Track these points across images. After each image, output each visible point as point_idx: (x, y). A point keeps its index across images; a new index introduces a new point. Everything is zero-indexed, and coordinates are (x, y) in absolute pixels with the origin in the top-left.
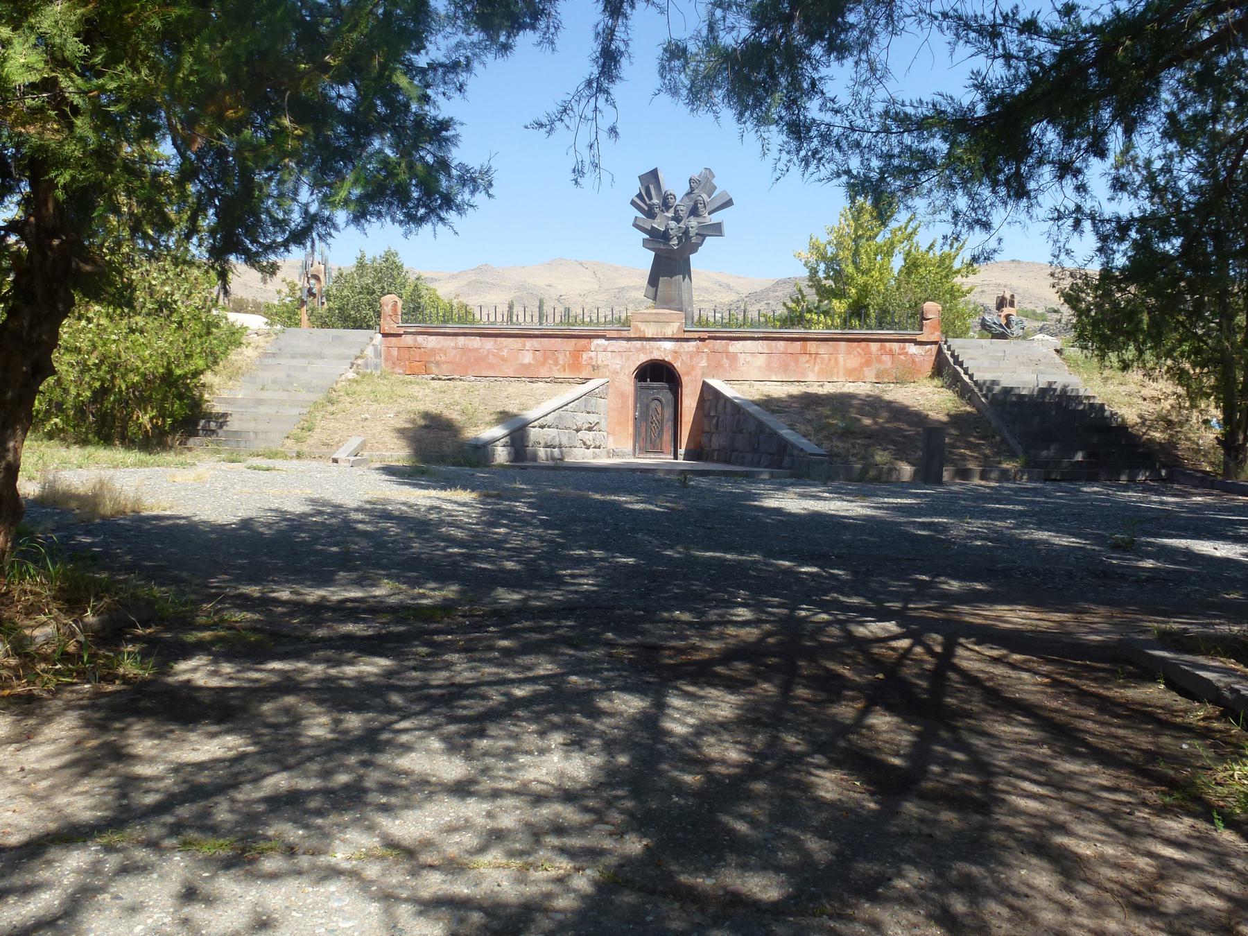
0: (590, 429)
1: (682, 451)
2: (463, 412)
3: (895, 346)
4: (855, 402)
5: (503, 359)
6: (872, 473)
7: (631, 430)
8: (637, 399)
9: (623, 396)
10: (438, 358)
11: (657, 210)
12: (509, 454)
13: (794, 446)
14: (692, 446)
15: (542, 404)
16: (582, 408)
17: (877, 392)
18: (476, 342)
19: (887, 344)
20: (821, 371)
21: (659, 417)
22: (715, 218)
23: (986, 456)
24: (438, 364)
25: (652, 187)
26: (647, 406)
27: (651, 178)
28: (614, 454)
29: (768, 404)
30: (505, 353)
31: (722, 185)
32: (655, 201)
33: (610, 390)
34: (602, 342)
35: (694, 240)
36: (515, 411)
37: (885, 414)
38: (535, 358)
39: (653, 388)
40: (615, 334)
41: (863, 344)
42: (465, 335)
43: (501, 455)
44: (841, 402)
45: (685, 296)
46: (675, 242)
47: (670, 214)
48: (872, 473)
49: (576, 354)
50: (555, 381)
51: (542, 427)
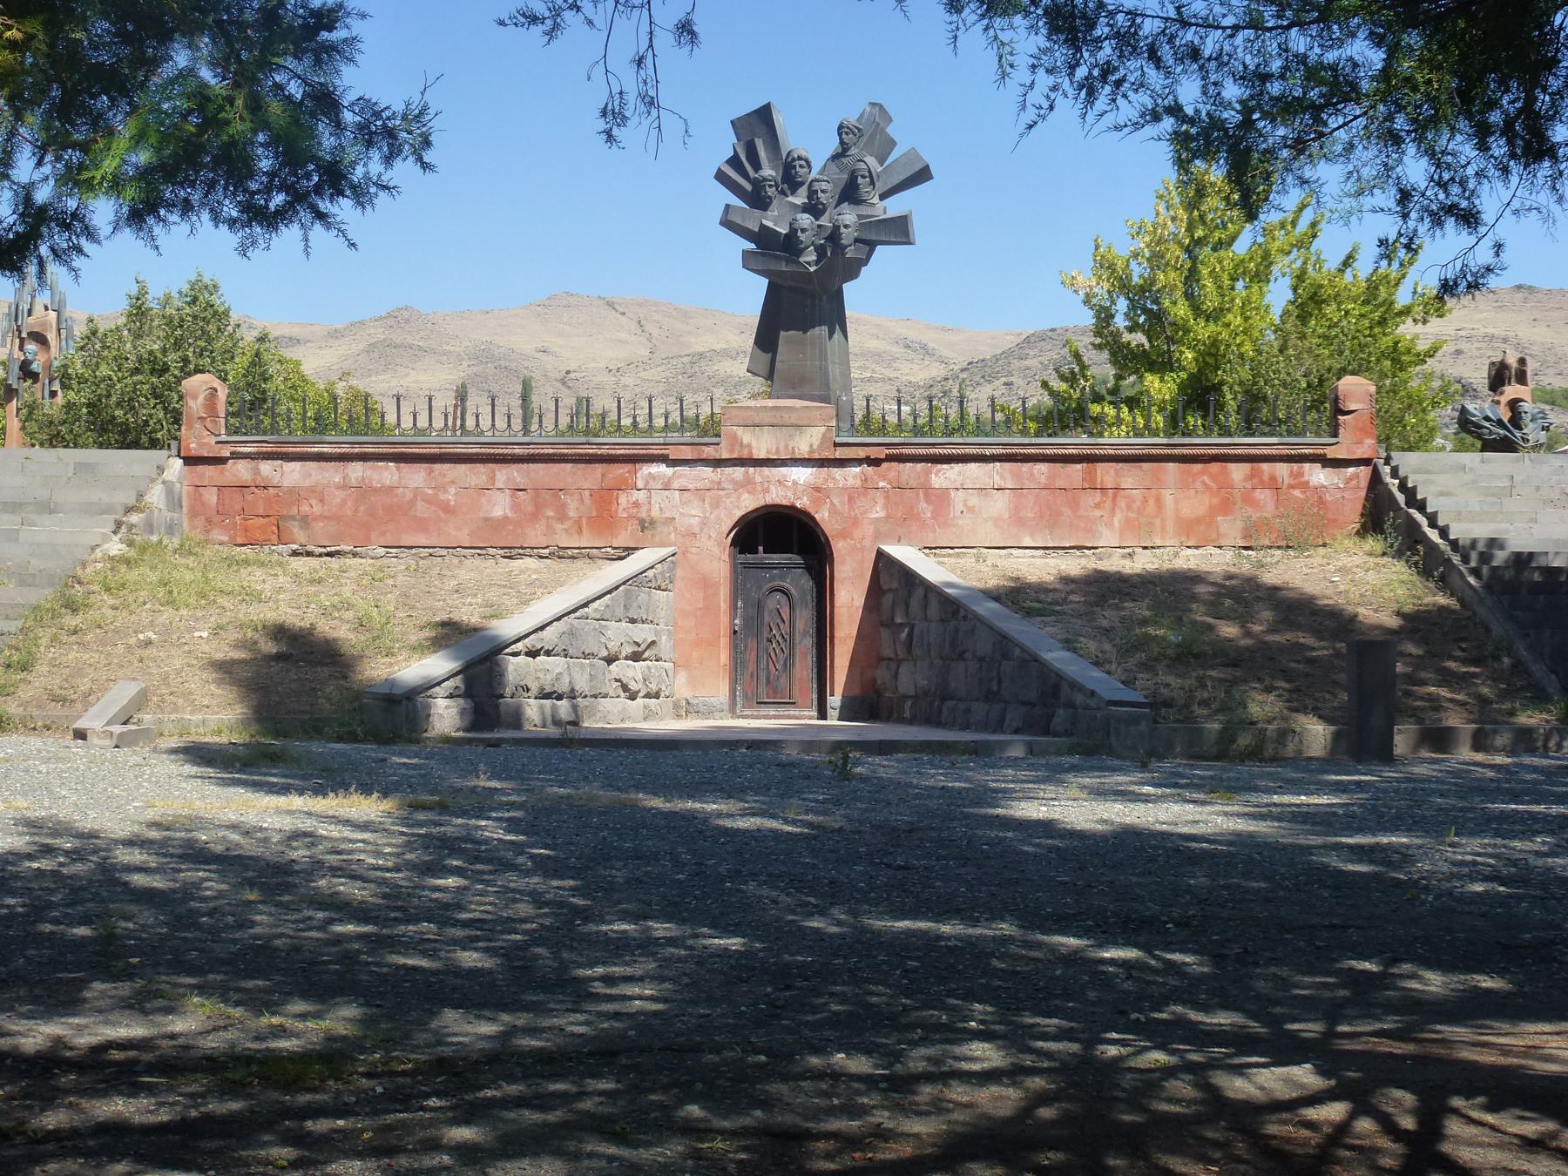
0: (636, 657)
1: (834, 701)
2: (361, 625)
3: (1282, 469)
4: (1201, 589)
5: (447, 509)
6: (1244, 740)
7: (724, 657)
8: (737, 590)
9: (705, 583)
10: (305, 509)
11: (771, 191)
12: (462, 712)
13: (1075, 686)
14: (856, 691)
15: (529, 604)
16: (620, 612)
17: (1246, 568)
18: (387, 473)
19: (1265, 466)
20: (1128, 525)
21: (785, 628)
22: (894, 207)
23: (1484, 701)
24: (305, 521)
25: (759, 144)
26: (760, 606)
27: (758, 125)
28: (689, 709)
29: (1017, 596)
30: (450, 496)
31: (908, 137)
32: (768, 172)
33: (679, 573)
34: (660, 469)
35: (850, 253)
36: (475, 620)
37: (1267, 614)
38: (516, 507)
39: (771, 567)
40: (687, 453)
41: (1214, 467)
42: (364, 457)
43: (445, 715)
44: (1172, 589)
45: (834, 370)
46: (810, 256)
47: (800, 199)
48: (1244, 740)
49: (605, 497)
50: (560, 554)
51: (533, 654)
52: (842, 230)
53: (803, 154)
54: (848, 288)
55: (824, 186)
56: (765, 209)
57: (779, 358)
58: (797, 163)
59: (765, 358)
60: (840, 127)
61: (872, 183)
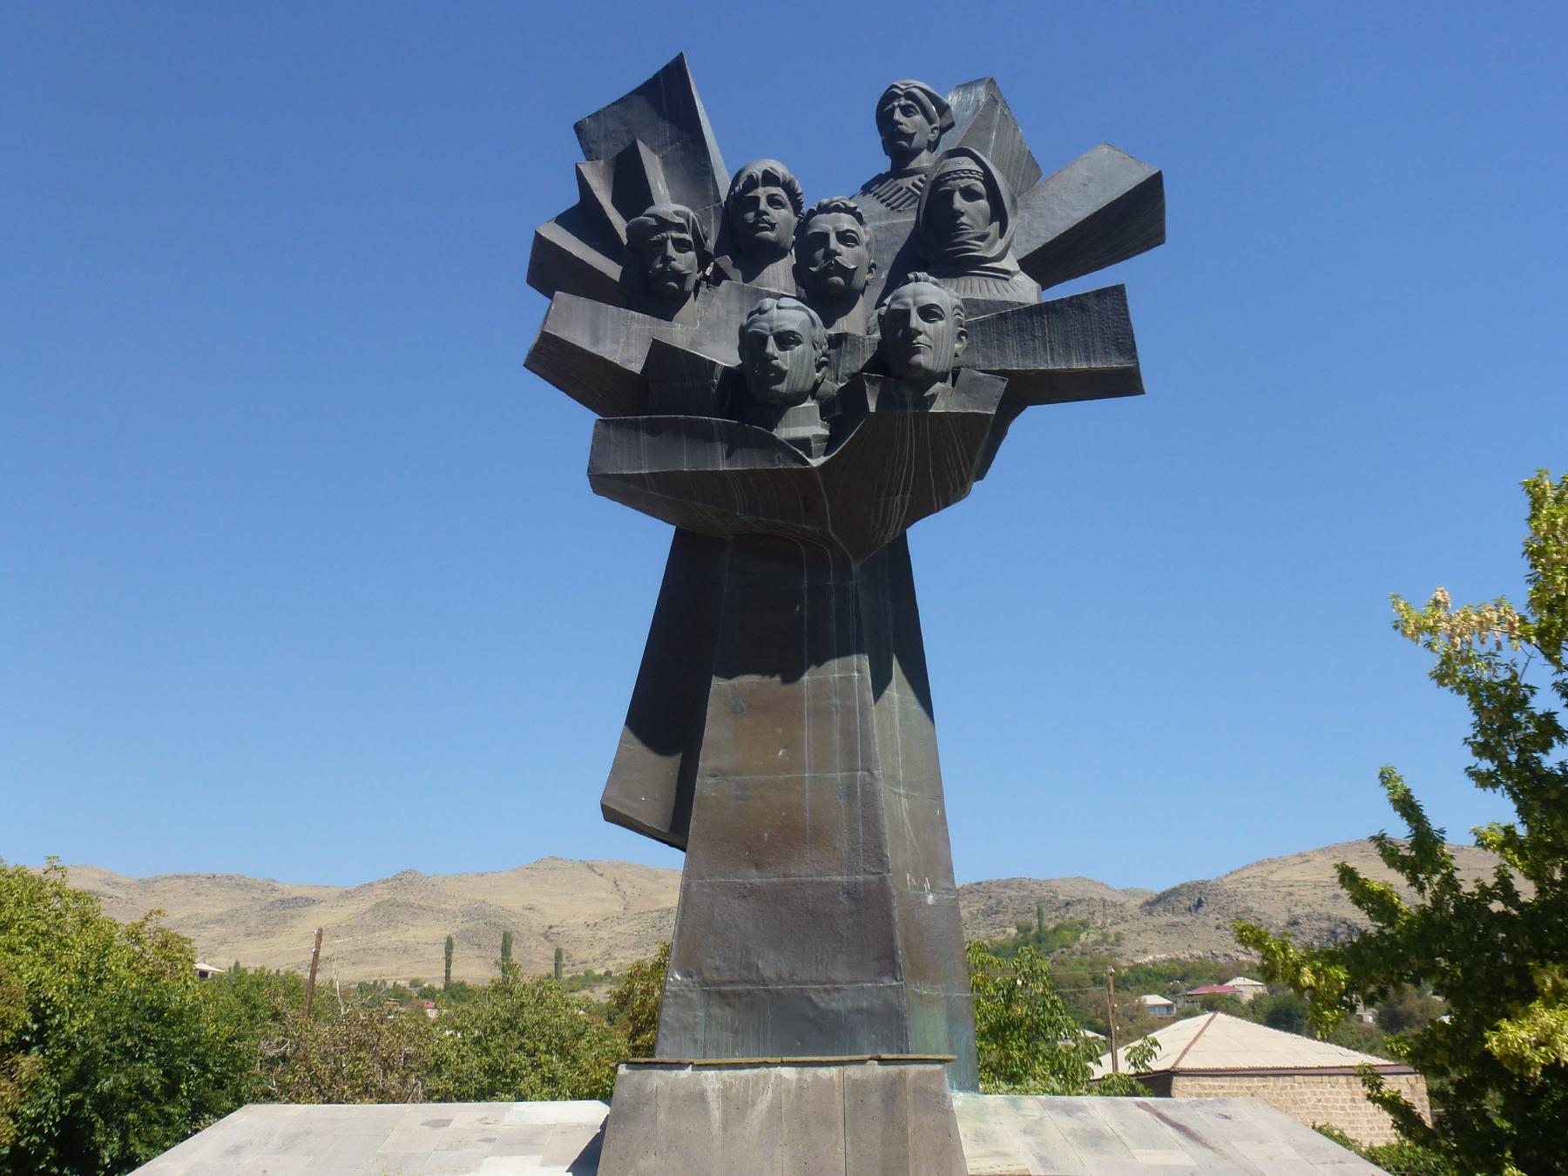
11: (684, 261)
35: (944, 400)
45: (897, 805)
47: (779, 275)
52: (916, 321)
53: (781, 170)
54: (929, 541)
55: (846, 222)
56: (669, 318)
57: (706, 763)
58: (762, 192)
59: (661, 769)
60: (889, 97)
61: (998, 213)
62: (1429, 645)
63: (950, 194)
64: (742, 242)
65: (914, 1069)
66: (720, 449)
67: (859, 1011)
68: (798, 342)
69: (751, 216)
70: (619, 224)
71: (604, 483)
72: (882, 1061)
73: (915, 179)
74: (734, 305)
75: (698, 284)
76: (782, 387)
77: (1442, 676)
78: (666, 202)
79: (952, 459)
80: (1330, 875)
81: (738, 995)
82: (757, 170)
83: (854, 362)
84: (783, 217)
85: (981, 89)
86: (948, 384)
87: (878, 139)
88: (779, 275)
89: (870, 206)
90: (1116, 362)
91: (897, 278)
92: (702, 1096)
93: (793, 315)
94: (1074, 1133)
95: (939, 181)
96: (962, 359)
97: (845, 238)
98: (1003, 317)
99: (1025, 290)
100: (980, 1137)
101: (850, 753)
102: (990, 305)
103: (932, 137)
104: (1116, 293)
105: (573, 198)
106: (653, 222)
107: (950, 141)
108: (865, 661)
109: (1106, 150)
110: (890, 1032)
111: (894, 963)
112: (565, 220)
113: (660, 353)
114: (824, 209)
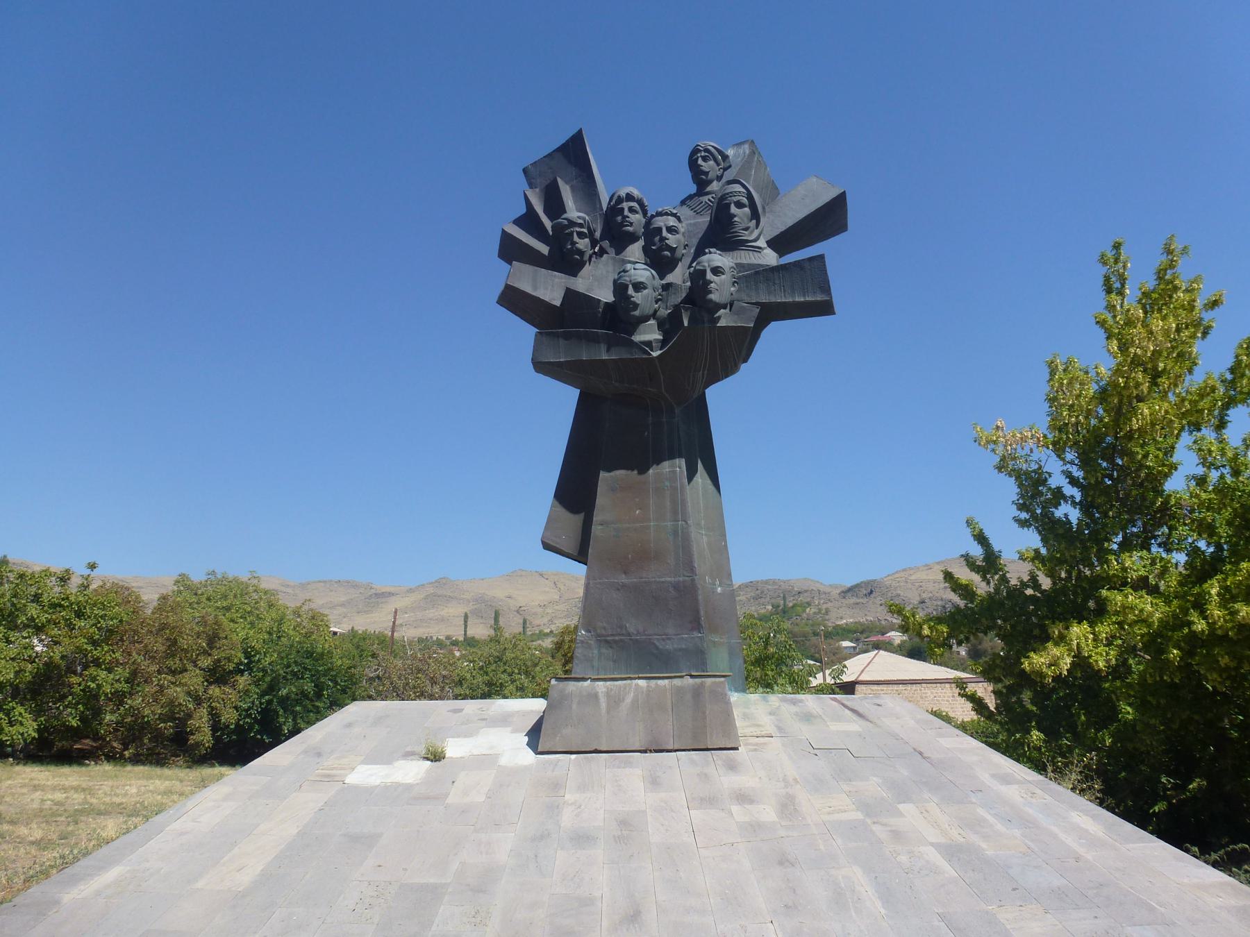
11: (583, 244)
35: (725, 319)
45: (701, 540)
46: (649, 333)
47: (635, 251)
52: (709, 276)
53: (636, 193)
55: (672, 221)
57: (598, 517)
58: (625, 205)
60: (695, 151)
61: (755, 215)
62: (993, 450)
63: (728, 205)
64: (615, 234)
65: (709, 681)
66: (603, 347)
67: (680, 650)
68: (645, 288)
69: (619, 218)
70: (548, 224)
71: (541, 366)
72: (692, 676)
73: (710, 197)
74: (610, 268)
75: (591, 257)
76: (637, 313)
77: (1000, 468)
78: (573, 211)
79: (732, 351)
80: (941, 576)
81: (615, 642)
82: (623, 193)
83: (677, 298)
84: (637, 219)
85: (746, 146)
86: (728, 310)
87: (689, 175)
88: (635, 251)
89: (685, 212)
90: (820, 297)
91: (700, 252)
92: (595, 696)
93: (642, 273)
94: (796, 714)
95: (723, 197)
96: (735, 296)
97: (671, 230)
98: (757, 273)
99: (770, 258)
100: (746, 716)
101: (675, 512)
102: (750, 266)
103: (719, 173)
104: (821, 258)
105: (522, 210)
106: (566, 222)
107: (729, 175)
108: (683, 462)
109: (815, 180)
110: (697, 661)
111: (699, 624)
112: (518, 222)
113: (570, 294)
114: (659, 214)
